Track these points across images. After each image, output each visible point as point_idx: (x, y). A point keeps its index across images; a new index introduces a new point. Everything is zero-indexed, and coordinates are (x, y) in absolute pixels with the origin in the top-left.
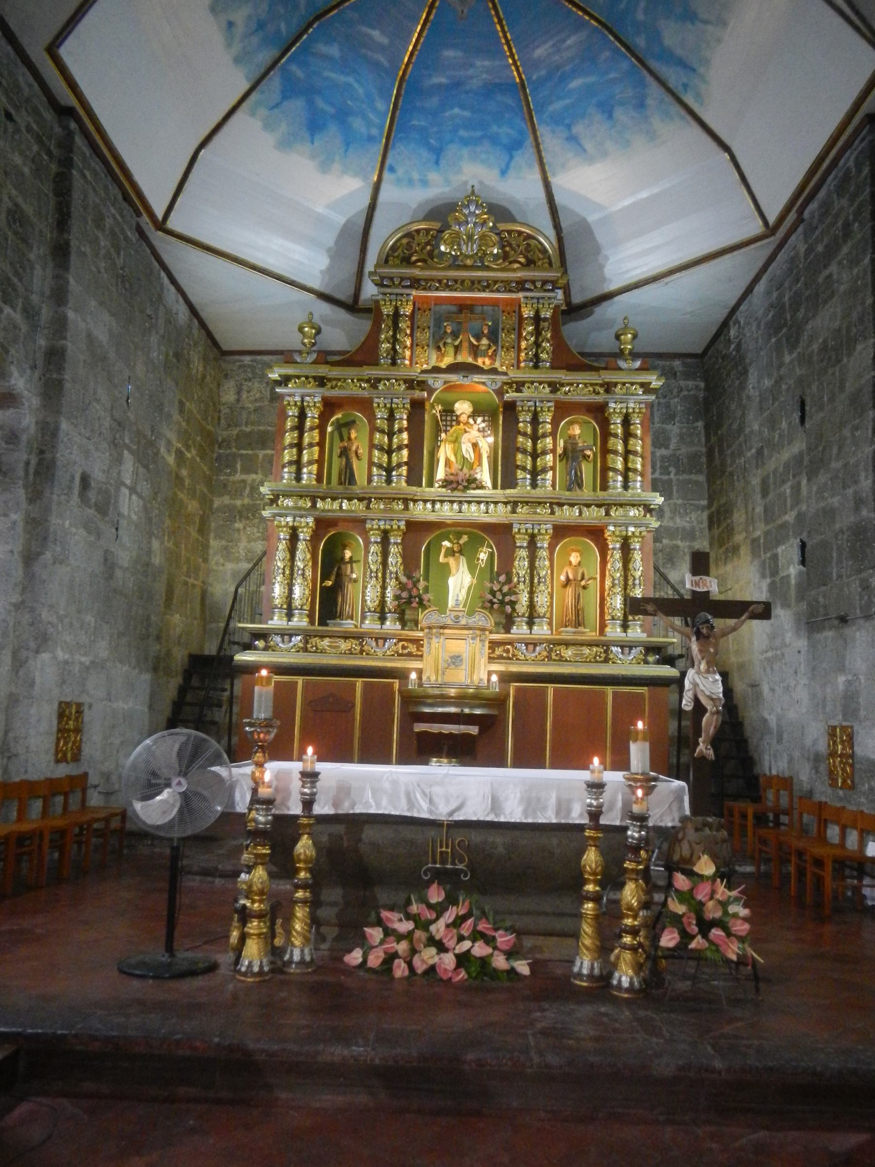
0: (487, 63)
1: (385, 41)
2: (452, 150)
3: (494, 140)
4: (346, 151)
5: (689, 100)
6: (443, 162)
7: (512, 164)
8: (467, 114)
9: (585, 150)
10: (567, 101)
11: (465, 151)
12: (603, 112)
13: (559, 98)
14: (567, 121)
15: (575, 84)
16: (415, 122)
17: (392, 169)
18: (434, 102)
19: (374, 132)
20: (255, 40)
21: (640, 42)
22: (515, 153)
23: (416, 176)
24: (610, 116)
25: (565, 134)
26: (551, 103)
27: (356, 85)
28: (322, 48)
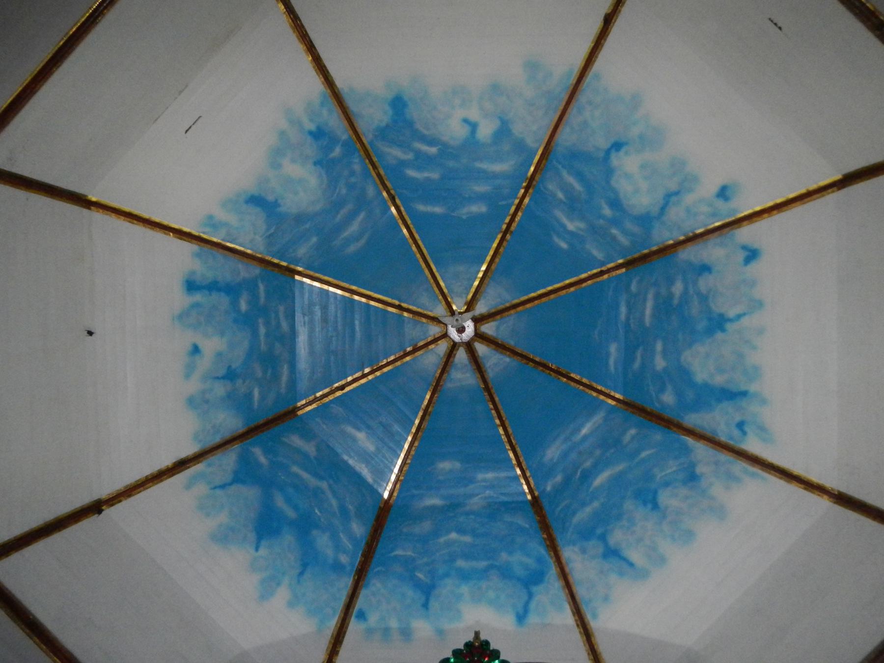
0: (490, 475)
1: (371, 447)
2: (447, 587)
3: (505, 573)
4: (301, 574)
5: (753, 445)
6: (434, 604)
7: (533, 605)
8: (468, 539)
9: (631, 565)
10: (596, 504)
11: (465, 589)
12: (645, 503)
13: (584, 504)
14: (599, 531)
15: (600, 480)
16: (399, 552)
17: (362, 616)
18: (426, 526)
19: (344, 559)
20: (220, 390)
21: (668, 398)
22: (535, 589)
23: (394, 624)
24: (655, 506)
25: (601, 550)
26: (574, 513)
27: (329, 495)
28: (296, 441)
